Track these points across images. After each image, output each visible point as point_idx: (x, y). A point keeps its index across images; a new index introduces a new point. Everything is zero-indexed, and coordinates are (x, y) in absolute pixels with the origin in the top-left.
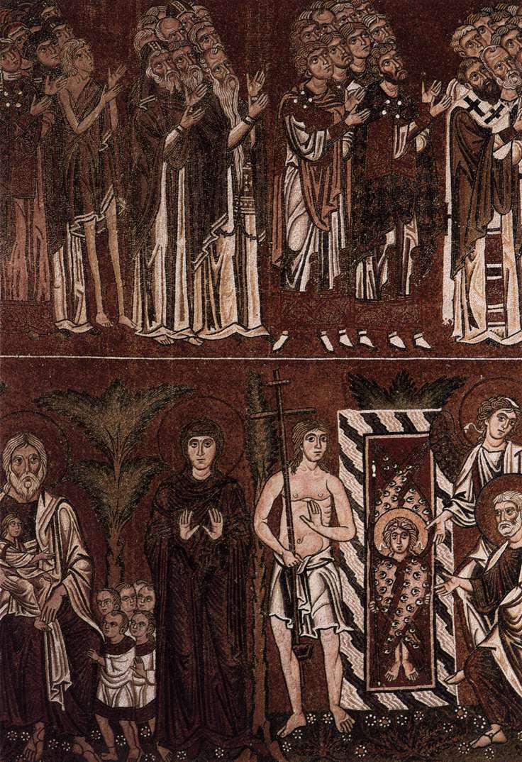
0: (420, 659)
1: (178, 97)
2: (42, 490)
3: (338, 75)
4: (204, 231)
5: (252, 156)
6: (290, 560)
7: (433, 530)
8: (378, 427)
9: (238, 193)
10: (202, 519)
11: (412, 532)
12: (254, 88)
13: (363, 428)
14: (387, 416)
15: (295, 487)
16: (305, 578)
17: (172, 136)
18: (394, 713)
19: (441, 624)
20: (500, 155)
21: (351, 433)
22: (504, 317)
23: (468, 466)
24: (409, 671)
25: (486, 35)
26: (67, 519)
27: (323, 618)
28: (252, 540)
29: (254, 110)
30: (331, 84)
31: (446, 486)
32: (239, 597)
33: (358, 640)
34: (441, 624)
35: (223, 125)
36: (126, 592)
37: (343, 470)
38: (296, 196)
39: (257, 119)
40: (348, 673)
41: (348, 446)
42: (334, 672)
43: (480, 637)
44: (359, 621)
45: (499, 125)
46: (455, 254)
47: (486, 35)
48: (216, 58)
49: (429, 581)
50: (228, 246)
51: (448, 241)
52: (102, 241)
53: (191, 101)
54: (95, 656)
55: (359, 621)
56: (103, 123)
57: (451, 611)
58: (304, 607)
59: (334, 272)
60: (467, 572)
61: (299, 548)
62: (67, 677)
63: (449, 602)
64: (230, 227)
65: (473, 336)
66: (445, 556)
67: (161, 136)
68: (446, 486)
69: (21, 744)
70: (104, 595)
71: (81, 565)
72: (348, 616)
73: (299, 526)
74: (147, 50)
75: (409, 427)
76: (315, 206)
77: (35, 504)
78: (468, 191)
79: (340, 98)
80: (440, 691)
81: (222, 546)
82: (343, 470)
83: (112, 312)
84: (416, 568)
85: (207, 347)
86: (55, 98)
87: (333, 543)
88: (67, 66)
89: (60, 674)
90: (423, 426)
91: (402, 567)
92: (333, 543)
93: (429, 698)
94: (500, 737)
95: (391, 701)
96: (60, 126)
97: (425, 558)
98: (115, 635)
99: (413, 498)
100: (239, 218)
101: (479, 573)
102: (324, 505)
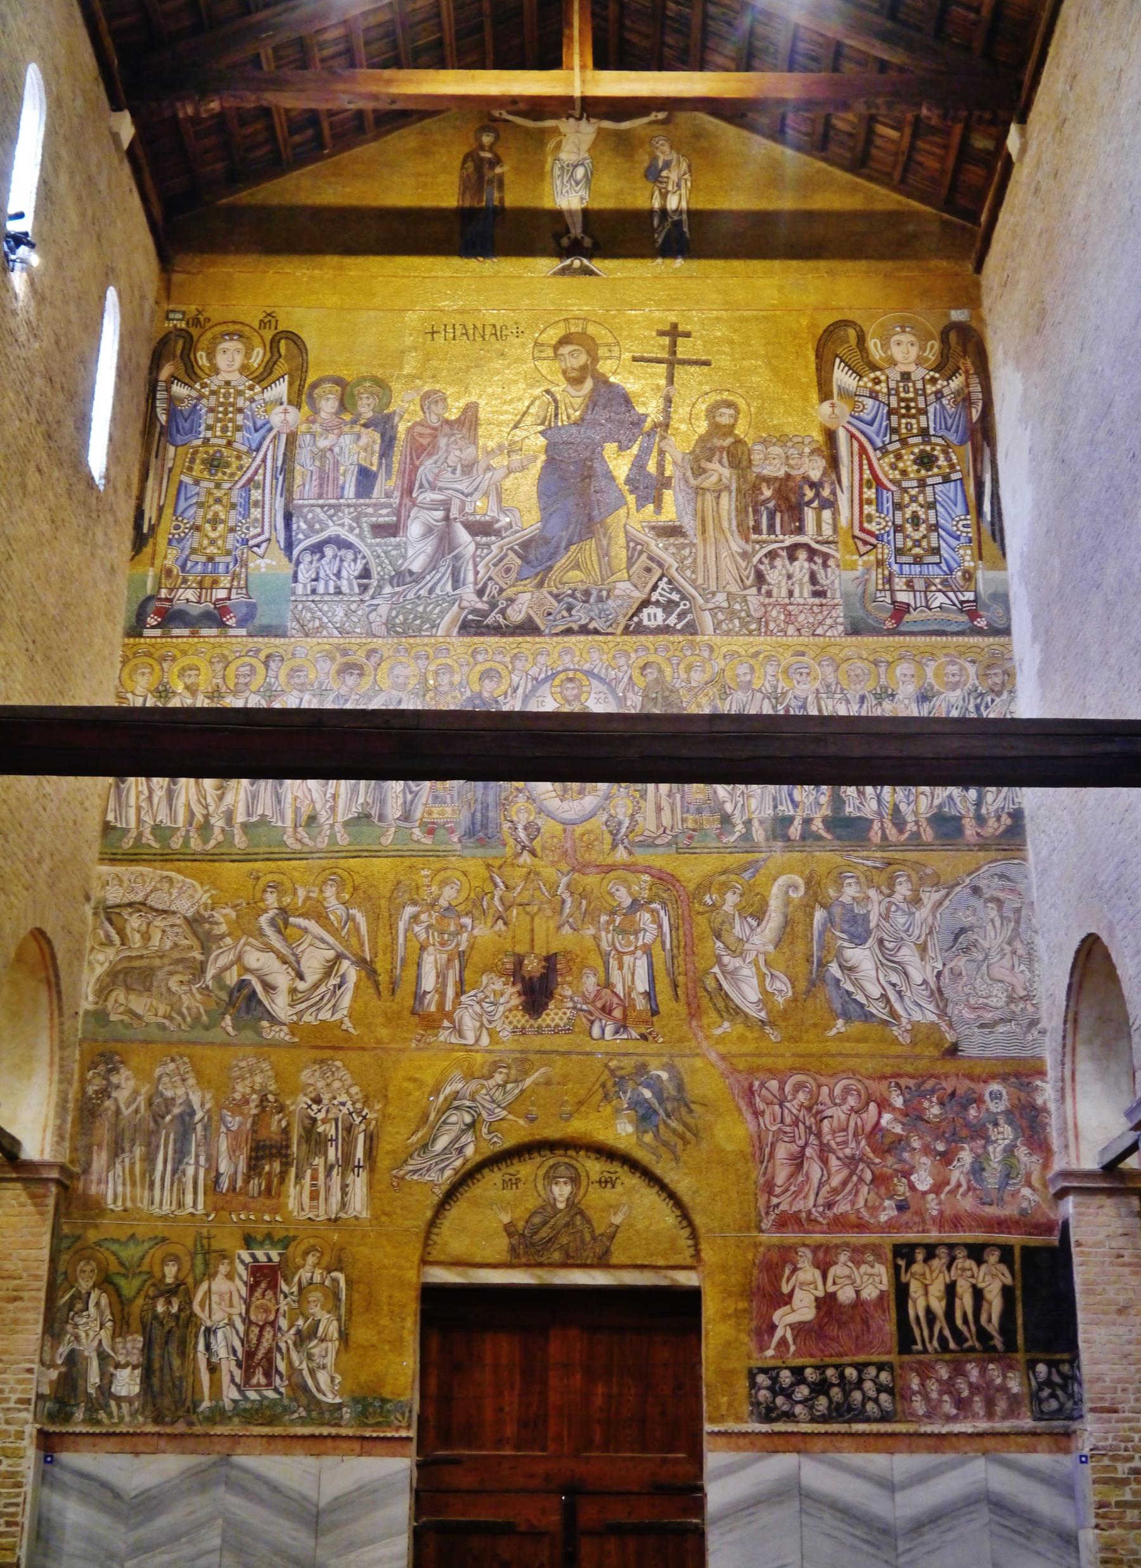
0: (267, 1374)
1: (173, 1099)
2: (94, 1287)
3: (248, 1090)
4: (180, 1162)
5: (205, 1128)
6: (209, 1323)
7: (277, 1310)
8: (255, 1259)
9: (198, 1146)
10: (169, 1303)
11: (267, 1311)
12: (208, 1096)
13: (248, 1259)
14: (260, 1255)
15: (214, 1287)
16: (215, 1332)
17: (168, 1118)
18: (253, 1401)
19: (279, 1356)
20: (320, 1130)
21: (242, 1262)
22: (317, 1207)
23: (296, 1279)
24: (263, 1381)
25: (317, 1074)
26: (104, 1300)
27: (222, 1352)
28: (193, 1314)
29: (208, 1106)
30: (243, 1096)
31: (285, 1288)
32: (183, 1342)
33: (239, 1365)
34: (279, 1356)
35: (193, 1113)
36: (129, 1338)
37: (237, 1279)
38: (224, 1144)
39: (209, 1111)
40: (233, 1381)
41: (241, 1269)
42: (226, 1379)
43: (297, 1363)
44: (240, 1354)
45: (320, 1116)
46: (297, 1176)
47: (317, 1074)
48: (192, 1081)
49: (275, 1335)
50: (190, 1171)
51: (293, 1170)
52: (132, 1165)
53: (179, 1101)
54: (112, 1370)
55: (240, 1354)
56: (137, 1111)
57: (284, 1350)
58: (214, 1347)
59: (239, 1183)
60: (293, 1331)
61: (214, 1318)
62: (98, 1380)
63: (283, 1346)
64: (192, 1161)
65: (303, 1216)
66: (283, 1323)
67: (163, 1117)
68: (285, 1288)
69: (72, 1414)
70: (119, 1340)
71: (109, 1324)
72: (235, 1352)
73: (214, 1306)
74: (160, 1078)
75: (270, 1260)
76: (233, 1152)
77: (89, 1294)
78: (304, 1147)
79: (247, 1102)
80: (276, 1390)
81: (177, 1317)
82: (237, 1279)
83: (133, 1200)
84: (268, 1328)
85: (175, 1219)
86: (116, 1099)
87: (230, 1315)
88: (123, 1084)
89: (94, 1378)
90: (276, 1258)
91: (262, 1328)
92: (230, 1315)
93: (271, 1394)
94: (304, 1414)
95: (252, 1395)
96: (118, 1112)
97: (273, 1324)
98: (122, 1359)
99: (269, 1295)
100: (197, 1156)
101: (299, 1332)
102: (227, 1297)
